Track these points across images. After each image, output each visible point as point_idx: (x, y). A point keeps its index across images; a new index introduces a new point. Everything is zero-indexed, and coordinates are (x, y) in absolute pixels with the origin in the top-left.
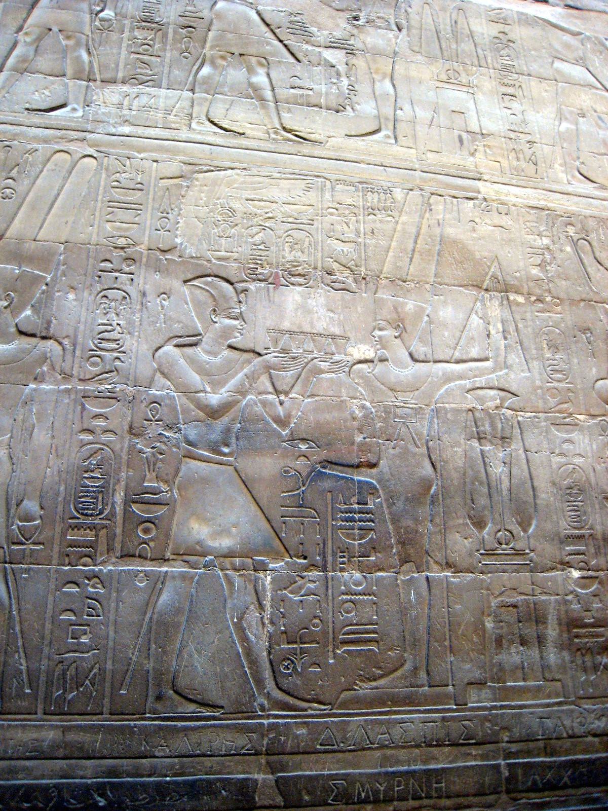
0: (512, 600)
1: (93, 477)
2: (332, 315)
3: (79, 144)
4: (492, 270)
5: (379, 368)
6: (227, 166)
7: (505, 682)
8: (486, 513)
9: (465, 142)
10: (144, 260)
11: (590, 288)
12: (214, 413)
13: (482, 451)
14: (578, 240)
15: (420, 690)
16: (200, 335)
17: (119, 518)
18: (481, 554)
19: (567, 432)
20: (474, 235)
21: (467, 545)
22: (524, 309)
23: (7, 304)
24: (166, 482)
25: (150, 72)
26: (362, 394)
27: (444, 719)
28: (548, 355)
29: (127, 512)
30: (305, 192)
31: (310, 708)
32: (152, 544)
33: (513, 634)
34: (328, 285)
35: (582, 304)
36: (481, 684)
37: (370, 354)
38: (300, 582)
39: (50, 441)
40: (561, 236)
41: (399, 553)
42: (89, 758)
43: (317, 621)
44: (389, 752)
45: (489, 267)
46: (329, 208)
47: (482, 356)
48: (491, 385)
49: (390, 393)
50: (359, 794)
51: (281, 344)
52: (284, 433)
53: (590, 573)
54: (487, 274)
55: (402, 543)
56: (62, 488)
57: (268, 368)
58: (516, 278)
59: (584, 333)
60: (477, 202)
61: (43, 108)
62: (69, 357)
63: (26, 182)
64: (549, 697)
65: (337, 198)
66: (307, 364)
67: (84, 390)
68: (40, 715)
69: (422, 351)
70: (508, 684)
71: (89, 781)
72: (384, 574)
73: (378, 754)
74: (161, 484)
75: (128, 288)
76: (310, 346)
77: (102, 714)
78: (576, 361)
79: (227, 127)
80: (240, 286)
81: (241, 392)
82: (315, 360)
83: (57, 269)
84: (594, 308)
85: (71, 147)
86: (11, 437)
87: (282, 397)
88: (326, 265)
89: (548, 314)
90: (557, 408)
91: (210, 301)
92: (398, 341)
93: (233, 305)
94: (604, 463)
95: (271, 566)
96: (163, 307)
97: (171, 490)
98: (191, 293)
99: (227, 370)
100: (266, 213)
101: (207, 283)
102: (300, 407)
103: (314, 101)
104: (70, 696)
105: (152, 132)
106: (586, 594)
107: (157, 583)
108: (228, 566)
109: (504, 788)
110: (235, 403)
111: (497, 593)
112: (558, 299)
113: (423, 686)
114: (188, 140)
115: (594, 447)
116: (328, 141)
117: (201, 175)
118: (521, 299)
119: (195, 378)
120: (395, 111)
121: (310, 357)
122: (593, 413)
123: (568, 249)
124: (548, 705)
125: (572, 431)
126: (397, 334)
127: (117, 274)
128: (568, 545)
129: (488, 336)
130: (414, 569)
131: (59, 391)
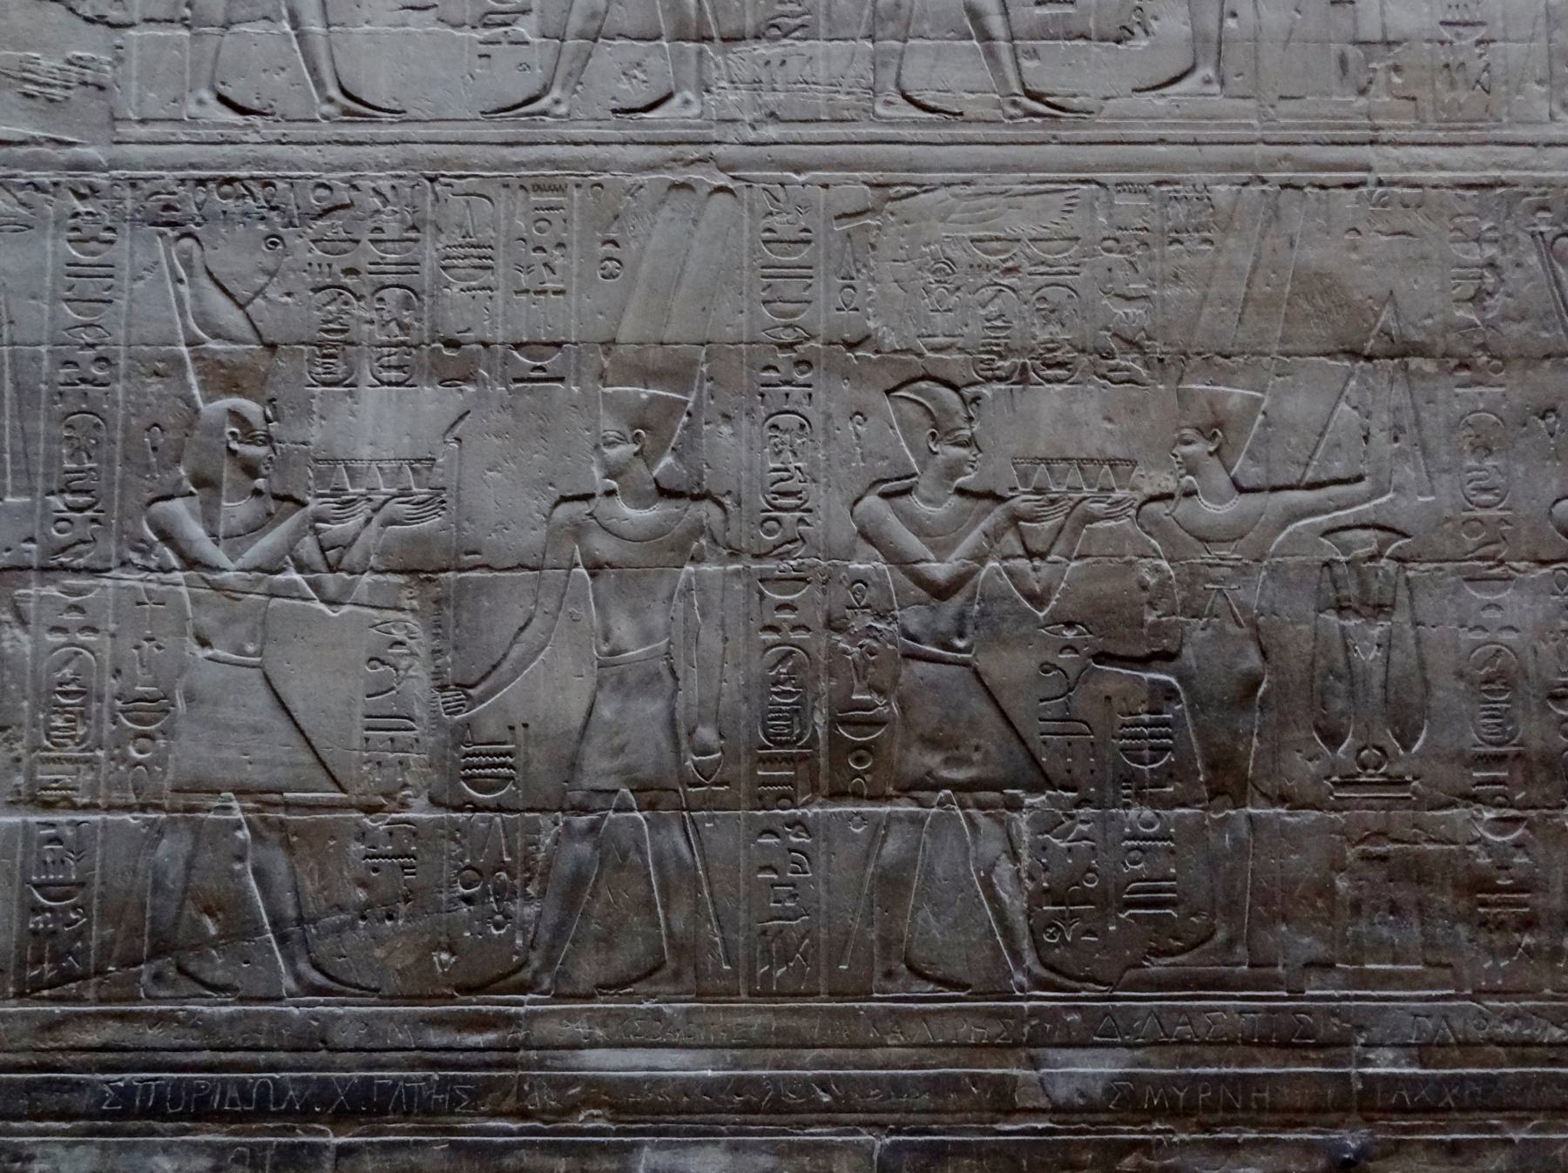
0: (1380, 849)
1: (784, 692)
2: (1109, 426)
3: (704, 168)
4: (1382, 319)
5: (1183, 507)
6: (937, 181)
7: (1362, 964)
8: (1344, 720)
9: (1351, 67)
10: (823, 361)
12: (941, 592)
13: (1343, 628)
15: (1238, 969)
16: (914, 475)
17: (822, 746)
18: (1334, 783)
20: (1354, 256)
21: (1313, 770)
23: (637, 448)
24: (881, 692)
25: (799, 9)
26: (1155, 550)
27: (1269, 1010)
28: (1471, 463)
29: (834, 740)
30: (1067, 216)
31: (1085, 989)
32: (868, 778)
33: (1379, 897)
34: (1104, 377)
35: (1547, 364)
36: (1326, 965)
37: (1171, 486)
38: (1068, 823)
39: (721, 645)
40: (1520, 235)
41: (1207, 783)
42: (807, 1047)
43: (1090, 875)
44: (1191, 1049)
45: (1377, 316)
46: (1105, 239)
47: (1355, 473)
48: (1365, 521)
49: (1199, 545)
50: (1150, 1100)
51: (1035, 479)
52: (1041, 615)
53: (1512, 812)
54: (1371, 328)
55: (1212, 766)
56: (744, 708)
57: (1015, 519)
58: (1424, 328)
59: (1543, 418)
60: (1363, 190)
61: (639, 106)
62: (732, 523)
63: (634, 246)
64: (1432, 987)
65: (1118, 220)
66: (1073, 508)
67: (761, 570)
68: (744, 996)
69: (1252, 473)
70: (1368, 966)
71: (809, 1073)
72: (1186, 811)
73: (1177, 1051)
74: (875, 696)
75: (806, 409)
76: (1075, 478)
77: (818, 993)
78: (1521, 468)
79: (932, 104)
80: (969, 392)
81: (980, 558)
82: (1085, 503)
83: (700, 388)
85: (693, 175)
86: (670, 643)
87: (1037, 563)
88: (1100, 343)
89: (1477, 389)
90: (1480, 552)
91: (926, 421)
92: (1214, 461)
93: (960, 422)
95: (1028, 801)
96: (858, 436)
97: (888, 704)
98: (897, 410)
99: (958, 525)
100: (1004, 261)
101: (919, 392)
102: (1064, 575)
103: (1077, 27)
104: (779, 972)
105: (814, 131)
107: (879, 830)
108: (970, 803)
109: (1355, 1104)
110: (971, 573)
111: (1357, 838)
112: (1501, 358)
113: (1239, 964)
114: (874, 138)
115: (1540, 615)
116: (1102, 108)
117: (898, 204)
118: (1429, 366)
119: (913, 544)
120: (1221, 20)
121: (1077, 496)
122: (1544, 557)
123: (1533, 259)
124: (1428, 999)
126: (1212, 449)
127: (787, 388)
128: (1478, 770)
129: (1366, 438)
130: (1230, 803)
131: (725, 574)
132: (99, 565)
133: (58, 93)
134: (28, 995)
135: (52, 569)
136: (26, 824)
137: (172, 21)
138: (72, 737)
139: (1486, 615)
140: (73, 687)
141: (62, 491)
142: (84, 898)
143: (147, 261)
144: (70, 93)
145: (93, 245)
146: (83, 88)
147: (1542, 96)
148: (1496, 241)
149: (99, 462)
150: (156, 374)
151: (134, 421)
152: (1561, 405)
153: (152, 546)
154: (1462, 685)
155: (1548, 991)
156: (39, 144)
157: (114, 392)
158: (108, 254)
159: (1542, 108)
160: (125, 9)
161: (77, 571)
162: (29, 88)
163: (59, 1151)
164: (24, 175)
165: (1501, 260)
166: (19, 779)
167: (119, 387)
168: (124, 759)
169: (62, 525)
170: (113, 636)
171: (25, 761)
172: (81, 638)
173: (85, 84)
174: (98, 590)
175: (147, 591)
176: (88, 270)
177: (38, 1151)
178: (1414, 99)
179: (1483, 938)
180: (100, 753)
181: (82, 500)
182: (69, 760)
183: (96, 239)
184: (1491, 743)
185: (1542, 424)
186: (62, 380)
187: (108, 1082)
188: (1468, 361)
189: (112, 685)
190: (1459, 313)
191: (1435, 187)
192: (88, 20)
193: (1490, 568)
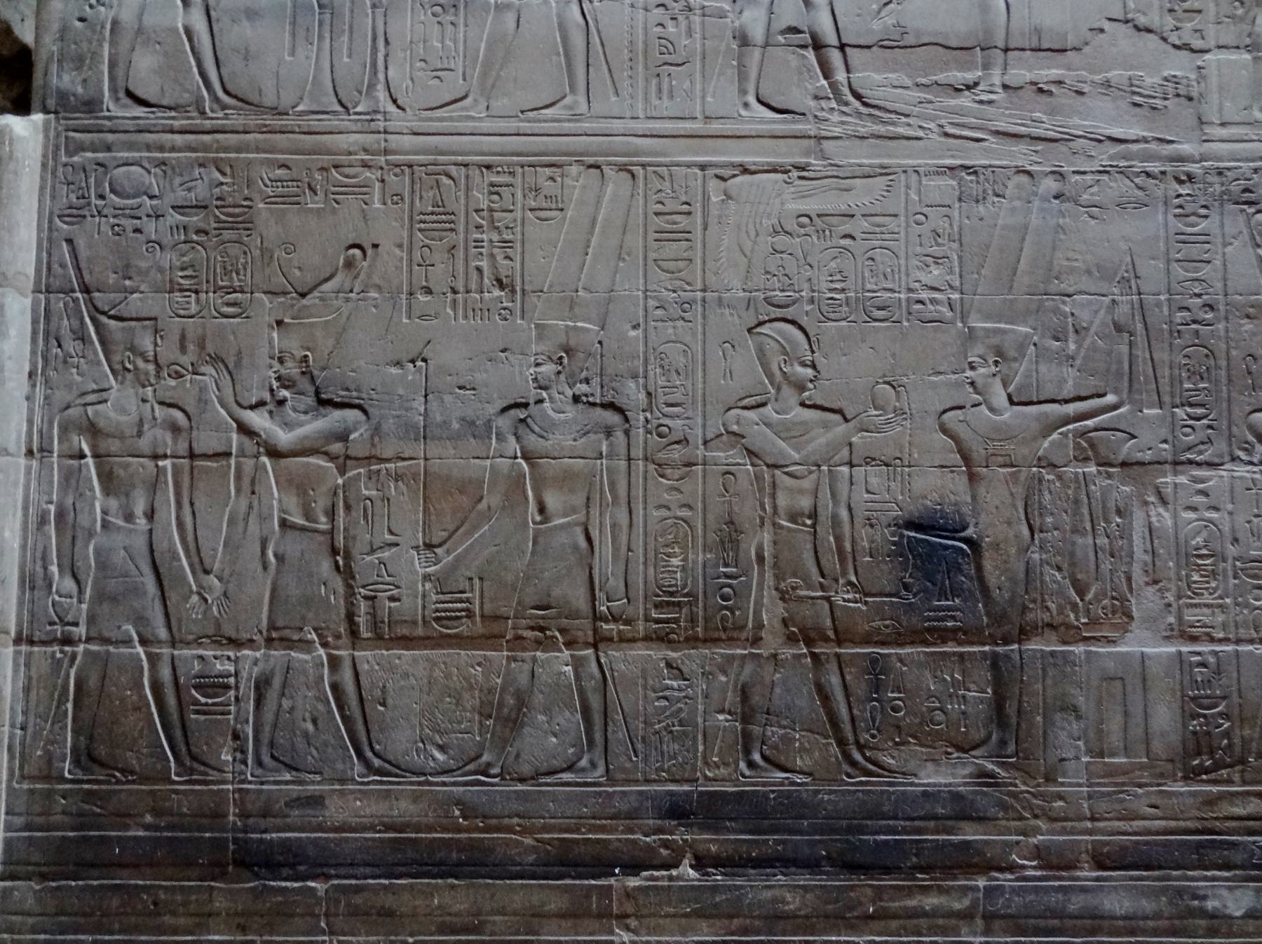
132: (1217, 460)
133: (1159, 103)
134: (1192, 779)
135: (1182, 463)
136: (1180, 653)
137: (1238, 47)
138: (1206, 589)
140: (1204, 552)
141: (1183, 405)
142: (1227, 706)
143: (1234, 231)
144: (1166, 103)
145: (1193, 219)
146: (1177, 100)
149: (1210, 382)
150: (1248, 317)
151: (1234, 353)
153: (1253, 447)
156: (1147, 142)
157: (1218, 330)
158: (1203, 225)
160: (1203, 38)
161: (1199, 464)
162: (1138, 99)
163: (1225, 893)
164: (1139, 166)
166: (1172, 619)
167: (1221, 326)
168: (1247, 605)
169: (1188, 430)
170: (1230, 513)
171: (1175, 605)
172: (1208, 515)
173: (1178, 95)
174: (1216, 479)
175: (1253, 479)
176: (1192, 238)
177: (1209, 893)
180: (1228, 600)
181: (1200, 411)
182: (1206, 605)
183: (1194, 214)
186: (1179, 321)
187: (1254, 842)
189: (1232, 550)
192: (1175, 46)
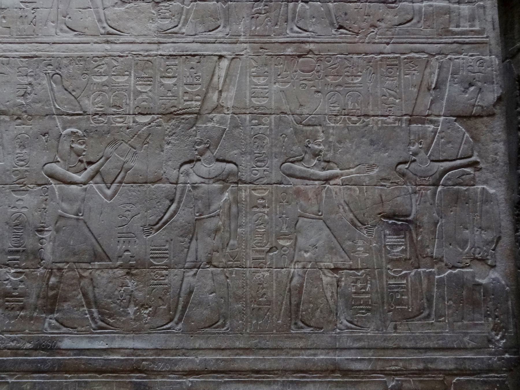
11: (54, 106)
14: (53, 75)
19: (21, 195)
22: (8, 124)
28: (18, 151)
35: (47, 117)
40: (41, 74)
53: (21, 270)
58: (6, 105)
59: (44, 136)
78: (35, 153)
84: (54, 119)
89: (23, 126)
90: (17, 182)
94: (40, 211)
106: (16, 280)
112: (31, 116)
115: (36, 202)
118: (7, 118)
122: (39, 183)
125: (25, 194)
139: (18, 203)
147: (53, 27)
148: (33, 76)
152: (50, 131)
154: (7, 227)
155: (27, 331)
159: (53, 31)
165: (34, 82)
178: (10, 28)
179: (7, 312)
184: (15, 247)
185: (43, 138)
188: (20, 117)
190: (18, 101)
191: (13, 57)
193: (21, 187)
